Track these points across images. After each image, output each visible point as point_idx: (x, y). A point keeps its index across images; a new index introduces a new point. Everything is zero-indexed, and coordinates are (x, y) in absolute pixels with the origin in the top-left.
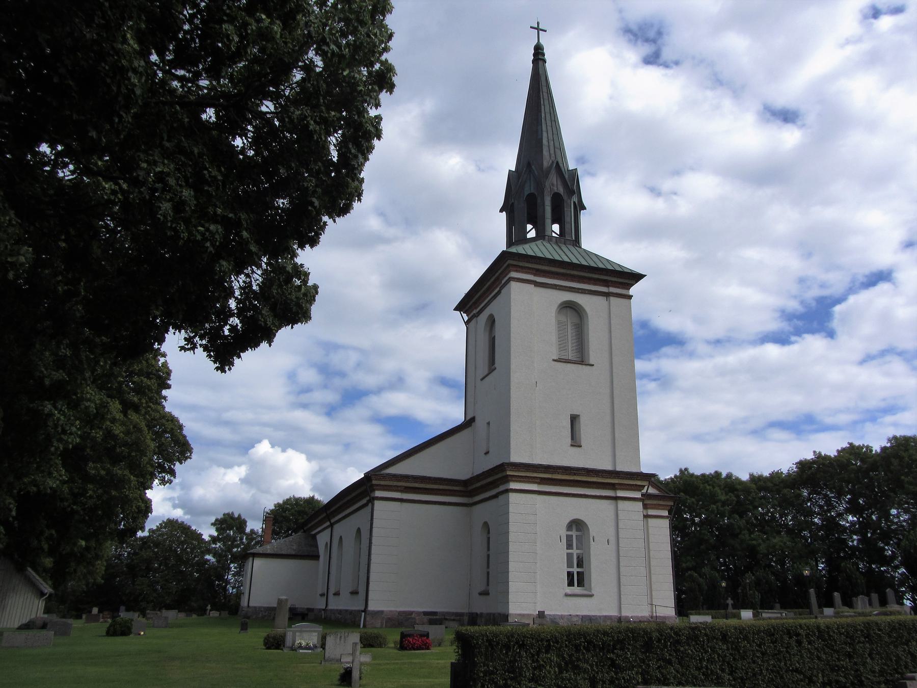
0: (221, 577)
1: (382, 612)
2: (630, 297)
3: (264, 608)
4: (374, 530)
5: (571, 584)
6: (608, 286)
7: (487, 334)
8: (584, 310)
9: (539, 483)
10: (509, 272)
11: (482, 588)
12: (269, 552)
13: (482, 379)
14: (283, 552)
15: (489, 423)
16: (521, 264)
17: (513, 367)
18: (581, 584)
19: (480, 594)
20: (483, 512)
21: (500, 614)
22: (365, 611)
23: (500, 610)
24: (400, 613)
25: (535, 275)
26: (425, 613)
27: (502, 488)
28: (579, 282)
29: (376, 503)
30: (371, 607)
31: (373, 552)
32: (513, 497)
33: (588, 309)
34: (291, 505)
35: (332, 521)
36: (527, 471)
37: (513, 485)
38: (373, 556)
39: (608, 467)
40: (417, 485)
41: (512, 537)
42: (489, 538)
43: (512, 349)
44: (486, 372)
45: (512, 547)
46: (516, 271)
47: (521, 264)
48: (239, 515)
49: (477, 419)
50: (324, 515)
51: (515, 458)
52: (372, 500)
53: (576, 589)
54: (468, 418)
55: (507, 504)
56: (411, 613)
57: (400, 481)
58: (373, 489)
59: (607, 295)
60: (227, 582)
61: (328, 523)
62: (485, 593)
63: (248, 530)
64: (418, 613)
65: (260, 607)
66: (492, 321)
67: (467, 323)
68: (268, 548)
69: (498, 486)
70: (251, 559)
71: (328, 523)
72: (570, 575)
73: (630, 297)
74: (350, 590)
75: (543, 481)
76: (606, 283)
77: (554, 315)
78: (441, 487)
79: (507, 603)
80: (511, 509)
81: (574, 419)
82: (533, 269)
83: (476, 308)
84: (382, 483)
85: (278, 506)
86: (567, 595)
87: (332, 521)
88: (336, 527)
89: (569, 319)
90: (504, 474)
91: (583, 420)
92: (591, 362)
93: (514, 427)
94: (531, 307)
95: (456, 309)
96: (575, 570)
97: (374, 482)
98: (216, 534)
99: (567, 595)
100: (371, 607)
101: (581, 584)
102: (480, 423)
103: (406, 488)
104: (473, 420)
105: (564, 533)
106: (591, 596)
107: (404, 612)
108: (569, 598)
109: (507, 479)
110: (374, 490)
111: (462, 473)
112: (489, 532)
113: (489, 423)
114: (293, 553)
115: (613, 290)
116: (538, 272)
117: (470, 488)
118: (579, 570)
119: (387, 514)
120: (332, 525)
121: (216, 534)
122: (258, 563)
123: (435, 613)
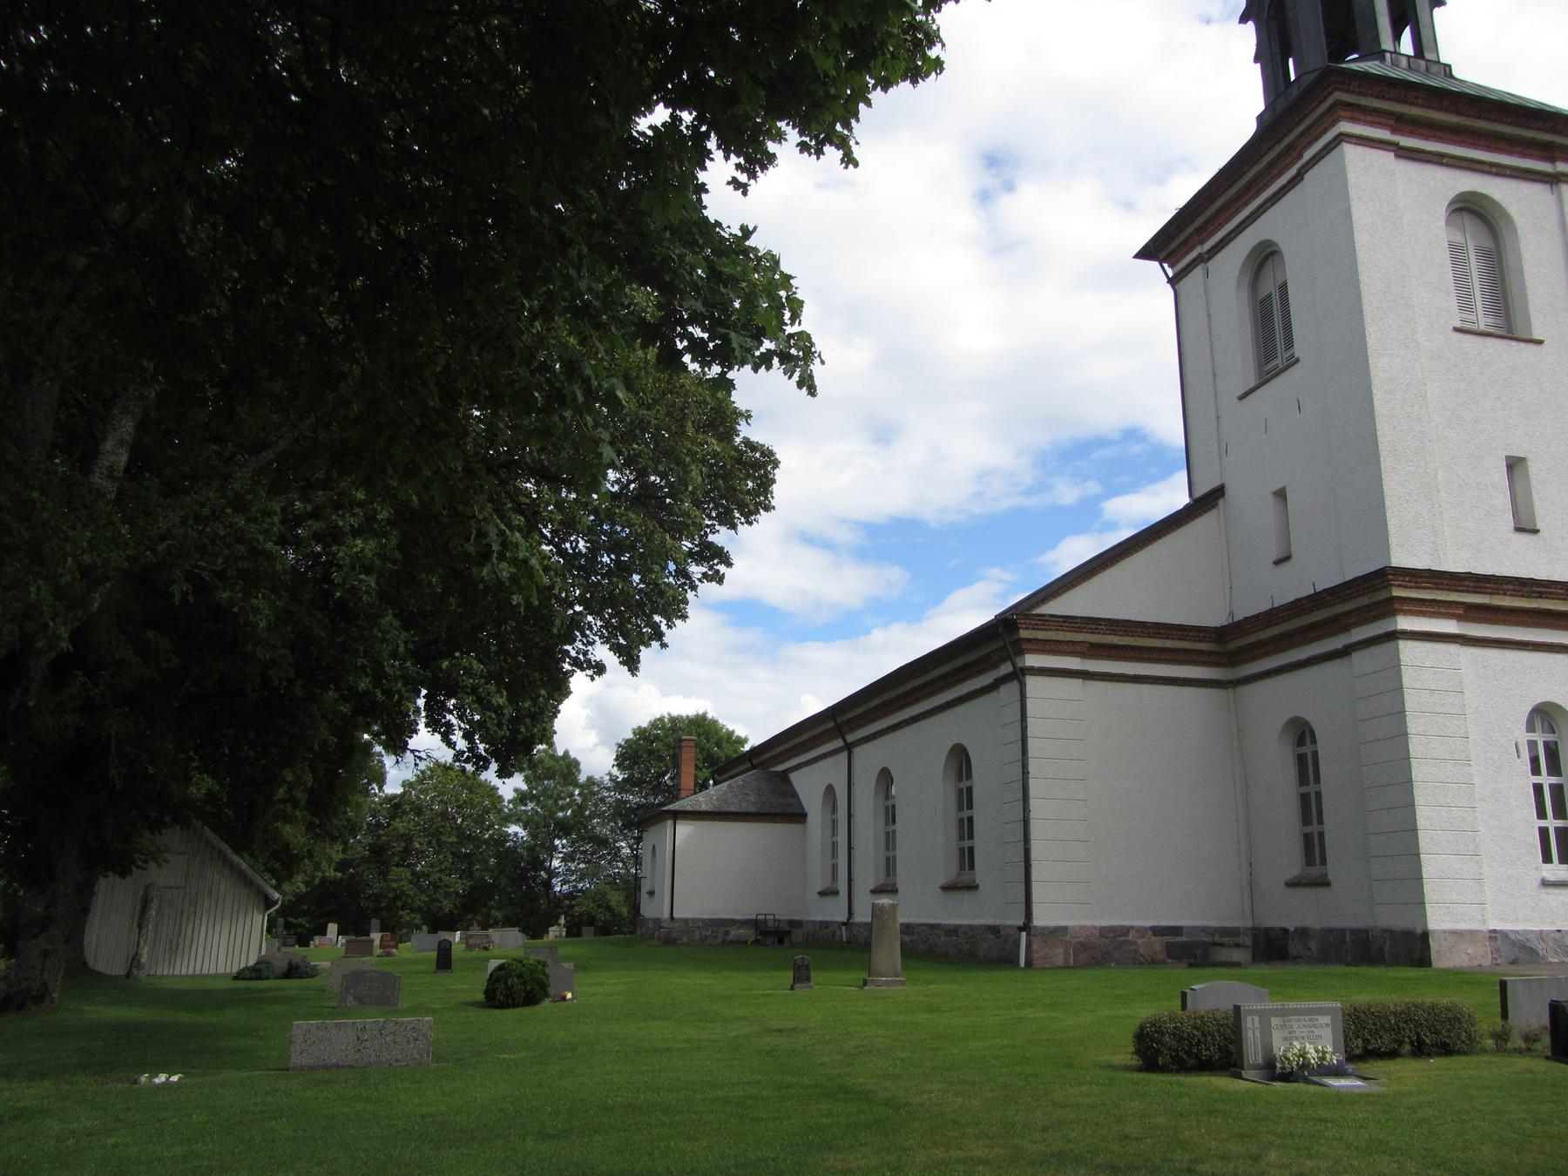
0: (538, 864)
1: (1064, 929)
3: (703, 921)
4: (1031, 743)
5: (1547, 858)
6: (1552, 160)
7: (1245, 296)
8: (1505, 215)
9: (1460, 618)
10: (1335, 122)
12: (704, 807)
13: (1241, 398)
14: (732, 809)
15: (1281, 494)
16: (1363, 101)
17: (1371, 342)
19: (1292, 884)
20: (1277, 699)
21: (1391, 932)
22: (1026, 927)
23: (1389, 918)
24: (1104, 932)
25: (1394, 130)
26: (1158, 931)
28: (1488, 149)
29: (1030, 681)
30: (1043, 918)
31: (1033, 792)
32: (1409, 651)
33: (1513, 211)
34: (663, 728)
35: (850, 738)
36: (1438, 587)
37: (1405, 623)
40: (1115, 640)
43: (1365, 300)
44: (1252, 384)
45: (1419, 771)
46: (1353, 120)
47: (1363, 101)
48: (566, 753)
49: (1229, 492)
50: (831, 724)
51: (1402, 557)
52: (1019, 675)
54: (1198, 494)
55: (1395, 666)
56: (1126, 930)
58: (1020, 648)
60: (552, 873)
61: (839, 743)
63: (582, 778)
64: (1142, 931)
65: (694, 920)
66: (1266, 255)
67: (1171, 281)
68: (702, 801)
69: (1347, 629)
70: (670, 823)
71: (839, 743)
74: (943, 881)
76: (1549, 152)
77: (1442, 223)
78: (1169, 644)
79: (1421, 904)
80: (1407, 680)
81: (1514, 465)
83: (1202, 243)
84: (1041, 635)
85: (641, 733)
86: (1545, 884)
87: (850, 738)
88: (858, 751)
89: (1472, 238)
90: (1381, 596)
91: (1536, 470)
94: (1388, 206)
95: (1147, 252)
97: (1024, 634)
98: (524, 787)
99: (1545, 884)
100: (1039, 920)
102: (1248, 499)
103: (1093, 646)
104: (1217, 494)
105: (1523, 737)
107: (1111, 929)
108: (1550, 890)
109: (1390, 608)
110: (1021, 653)
114: (753, 809)
116: (1401, 123)
117: (1233, 645)
119: (1061, 710)
120: (849, 747)
121: (524, 787)
122: (684, 829)
123: (1176, 930)
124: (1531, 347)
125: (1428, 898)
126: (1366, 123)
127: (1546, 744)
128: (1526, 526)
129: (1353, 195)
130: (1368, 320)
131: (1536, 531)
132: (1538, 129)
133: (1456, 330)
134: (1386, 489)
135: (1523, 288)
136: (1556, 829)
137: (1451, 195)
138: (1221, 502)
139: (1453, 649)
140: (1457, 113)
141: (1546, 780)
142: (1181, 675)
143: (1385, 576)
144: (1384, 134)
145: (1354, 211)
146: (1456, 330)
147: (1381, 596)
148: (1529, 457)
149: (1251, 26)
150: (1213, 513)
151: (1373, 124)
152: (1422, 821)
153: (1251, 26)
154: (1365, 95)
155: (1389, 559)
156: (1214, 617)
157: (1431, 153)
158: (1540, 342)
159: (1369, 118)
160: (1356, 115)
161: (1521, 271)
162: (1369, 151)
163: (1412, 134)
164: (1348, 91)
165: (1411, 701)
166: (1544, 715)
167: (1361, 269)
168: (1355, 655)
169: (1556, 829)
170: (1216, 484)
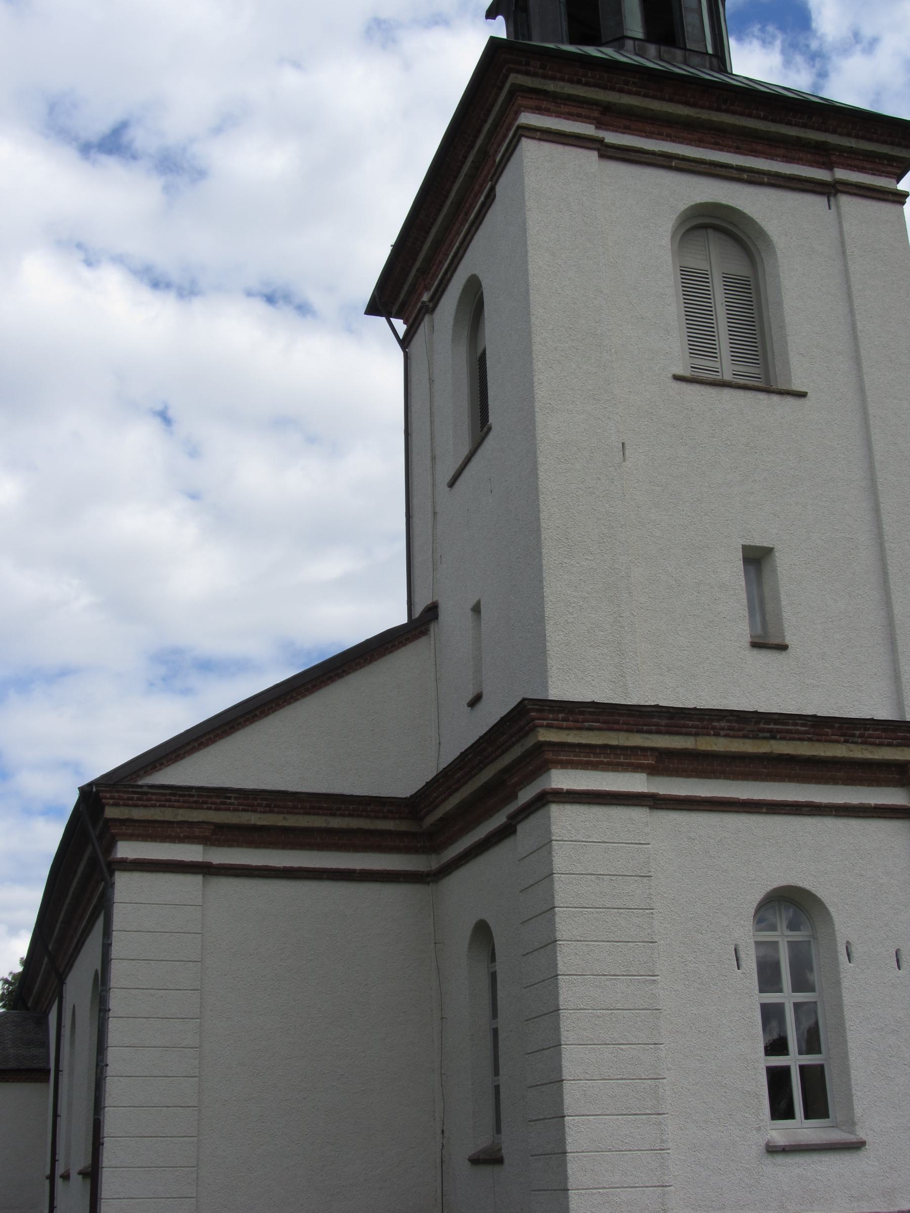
2: (900, 198)
5: (781, 1108)
6: (829, 166)
7: (463, 350)
8: (762, 234)
9: (652, 771)
10: (517, 114)
11: (483, 1142)
13: (451, 484)
15: (476, 609)
16: (551, 86)
17: (541, 393)
18: (817, 1107)
19: (475, 1161)
27: (526, 795)
28: (738, 150)
32: (564, 820)
33: (771, 227)
37: (562, 779)
38: (112, 1055)
39: (883, 713)
40: (253, 819)
41: (567, 958)
42: (493, 976)
45: (569, 993)
46: (539, 110)
47: (551, 86)
51: (563, 687)
53: (801, 1129)
55: (546, 845)
57: (197, 806)
59: (829, 190)
62: (489, 1158)
67: (405, 343)
72: (778, 1080)
73: (900, 198)
75: (664, 763)
76: (823, 155)
78: (336, 823)
81: (756, 559)
82: (594, 103)
84: (138, 814)
86: (773, 1150)
90: (529, 743)
91: (784, 564)
92: (797, 386)
93: (556, 588)
94: (591, 222)
96: (794, 1060)
97: (111, 812)
99: (773, 1150)
101: (817, 1107)
102: (453, 619)
103: (220, 828)
105: (745, 933)
106: (857, 1146)
108: (780, 1159)
109: (541, 759)
111: (400, 774)
112: (493, 958)
113: (476, 609)
115: (841, 174)
116: (608, 115)
118: (810, 1060)
124: (790, 400)
125: (572, 1182)
126: (559, 115)
127: (793, 946)
128: (766, 642)
129: (530, 203)
130: (538, 365)
131: (783, 648)
132: (805, 126)
133: (677, 378)
134: (547, 591)
135: (782, 327)
136: (802, 1068)
137: (682, 206)
138: (433, 627)
139: (639, 815)
140: (687, 104)
141: (787, 997)
142: (296, 864)
143: (528, 713)
144: (588, 129)
145: (530, 223)
146: (677, 378)
147: (529, 743)
148: (778, 547)
149: (500, 19)
150: (423, 641)
151: (570, 116)
152: (569, 1069)
153: (500, 19)
154: (553, 78)
155: (546, 689)
156: (404, 783)
157: (653, 153)
158: (802, 395)
159: (564, 109)
160: (544, 104)
161: (780, 304)
162: (560, 148)
163: (626, 130)
164: (527, 73)
165: (564, 891)
166: (790, 905)
167: (534, 297)
168: (520, 828)
169: (802, 1068)
170: (429, 602)
